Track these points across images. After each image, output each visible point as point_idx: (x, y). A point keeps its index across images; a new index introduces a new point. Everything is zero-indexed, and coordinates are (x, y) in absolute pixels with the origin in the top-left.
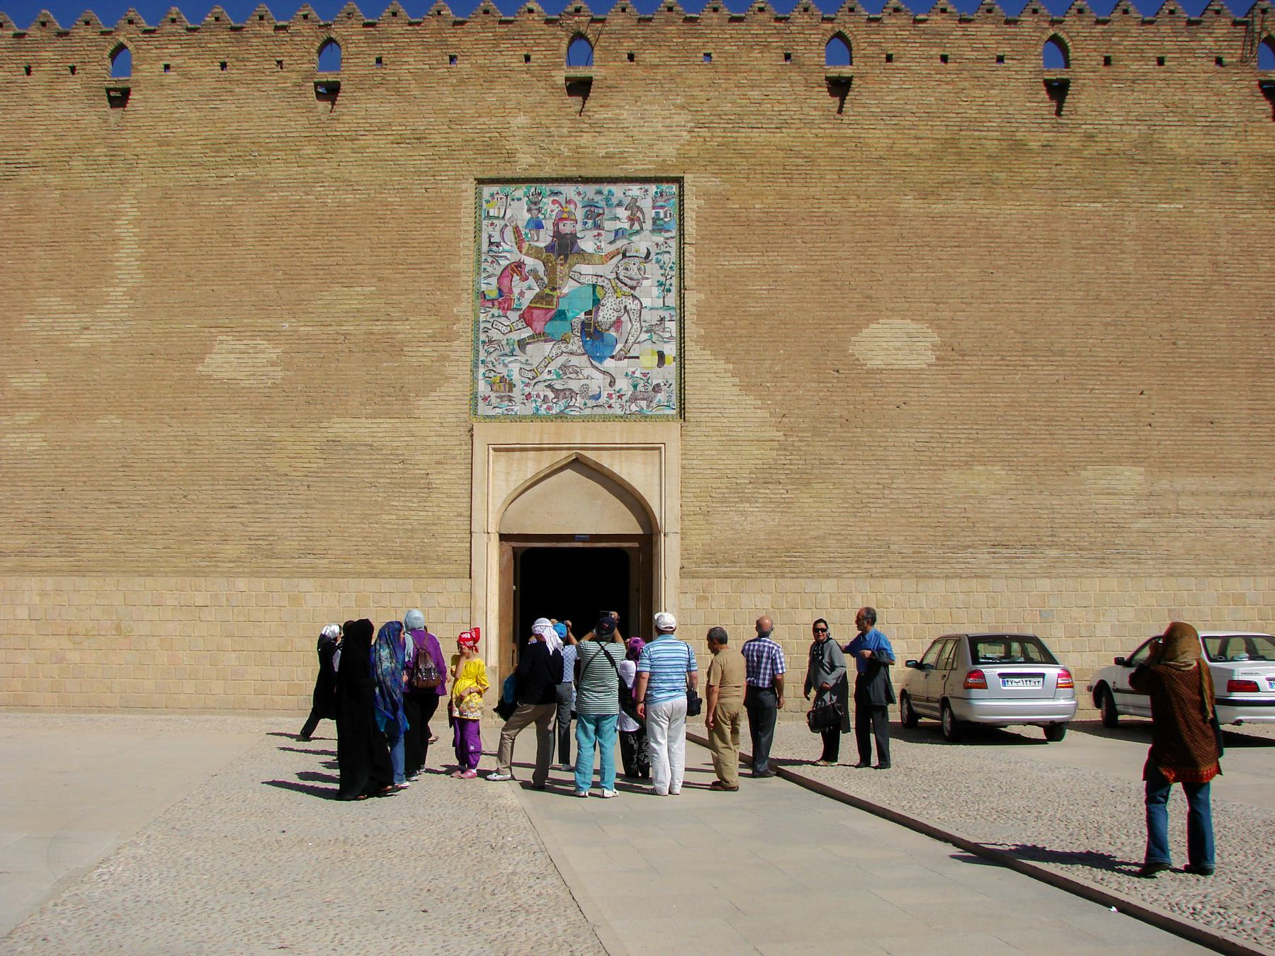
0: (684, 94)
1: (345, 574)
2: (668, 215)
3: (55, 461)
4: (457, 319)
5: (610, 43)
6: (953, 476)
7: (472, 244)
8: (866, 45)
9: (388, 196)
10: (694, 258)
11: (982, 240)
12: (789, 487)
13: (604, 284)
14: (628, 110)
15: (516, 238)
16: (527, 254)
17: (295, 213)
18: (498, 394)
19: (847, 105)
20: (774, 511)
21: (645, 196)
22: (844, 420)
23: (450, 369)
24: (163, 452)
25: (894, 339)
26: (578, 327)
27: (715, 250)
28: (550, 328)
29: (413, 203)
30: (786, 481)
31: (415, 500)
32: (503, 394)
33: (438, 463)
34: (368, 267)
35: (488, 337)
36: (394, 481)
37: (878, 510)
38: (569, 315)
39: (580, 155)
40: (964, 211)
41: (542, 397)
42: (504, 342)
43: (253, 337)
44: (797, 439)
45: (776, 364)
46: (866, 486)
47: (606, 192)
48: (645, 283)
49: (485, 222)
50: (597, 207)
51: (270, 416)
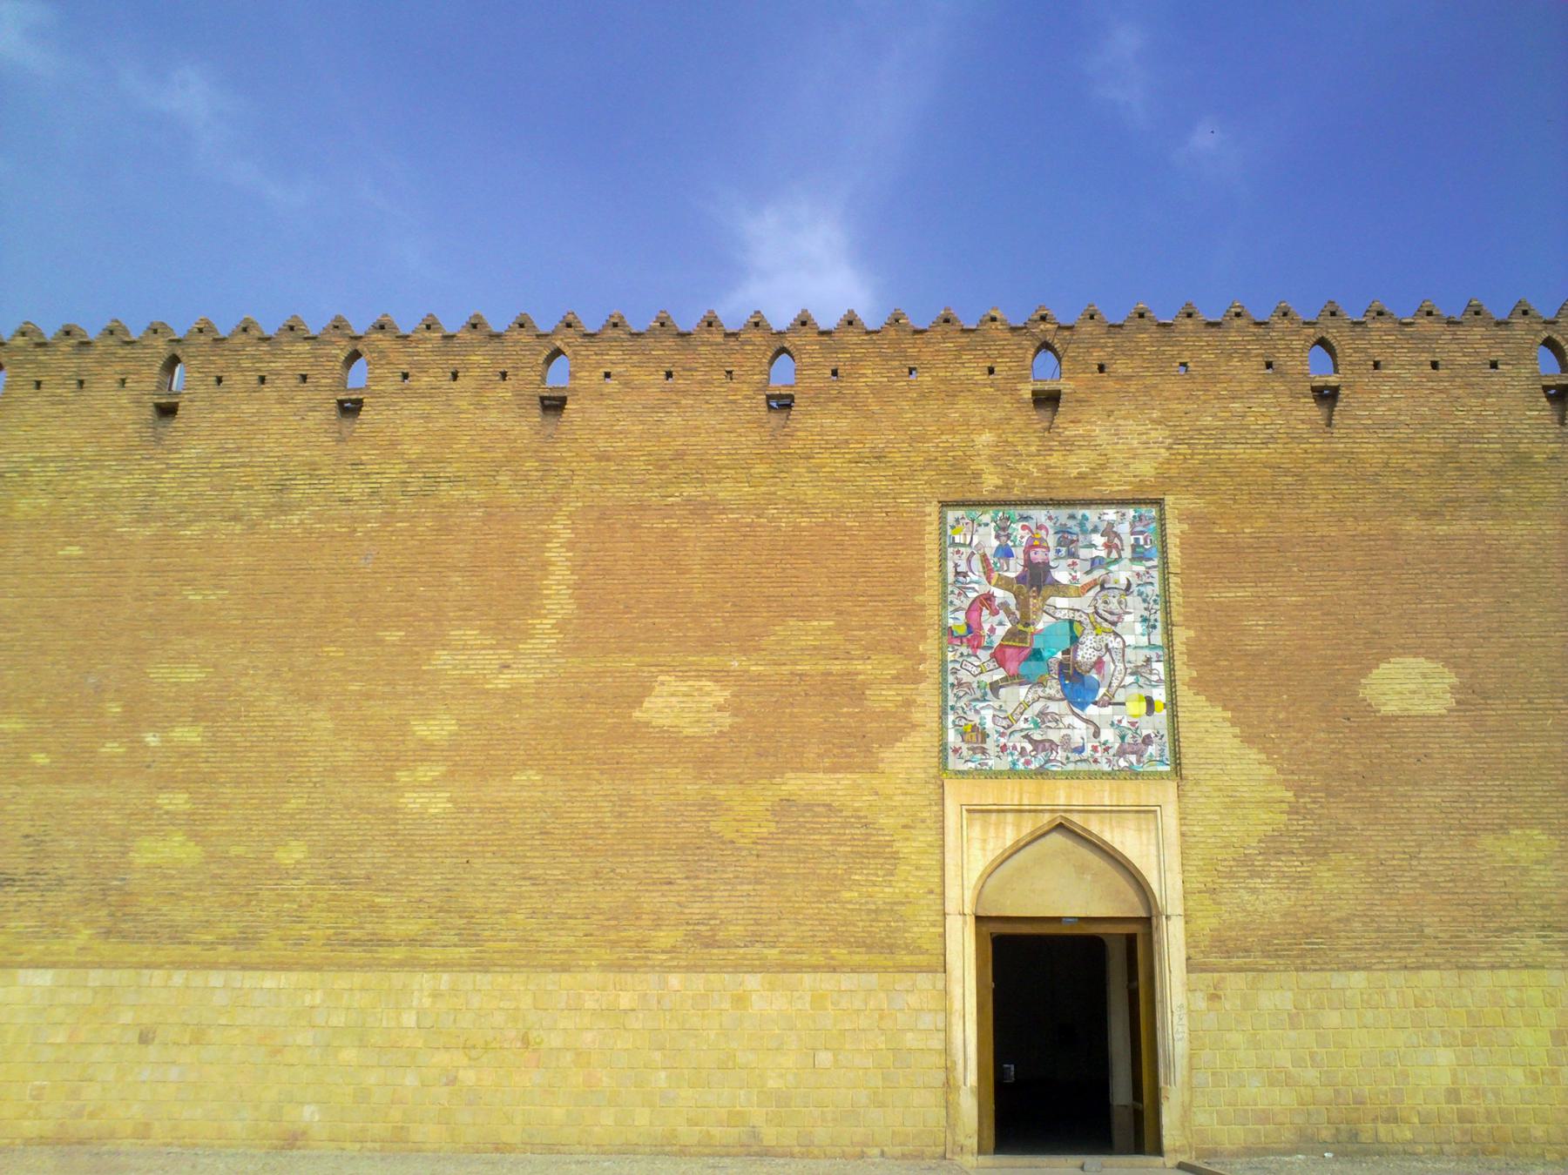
0: (1159, 407)
3: (461, 827)
4: (923, 658)
6: (1487, 841)
7: (937, 574)
10: (1180, 590)
11: (1494, 565)
12: (1305, 858)
13: (1082, 619)
14: (1101, 426)
15: (984, 568)
16: (996, 585)
19: (1336, 419)
20: (1288, 888)
22: (1360, 778)
23: (917, 716)
24: (590, 815)
26: (1055, 668)
27: (1202, 581)
30: (1300, 851)
33: (905, 827)
34: (825, 599)
35: (957, 679)
37: (1407, 885)
38: (1046, 654)
39: (1050, 476)
40: (1471, 532)
41: (1019, 749)
43: (698, 677)
44: (1309, 800)
46: (1391, 856)
48: (1127, 618)
51: (716, 770)
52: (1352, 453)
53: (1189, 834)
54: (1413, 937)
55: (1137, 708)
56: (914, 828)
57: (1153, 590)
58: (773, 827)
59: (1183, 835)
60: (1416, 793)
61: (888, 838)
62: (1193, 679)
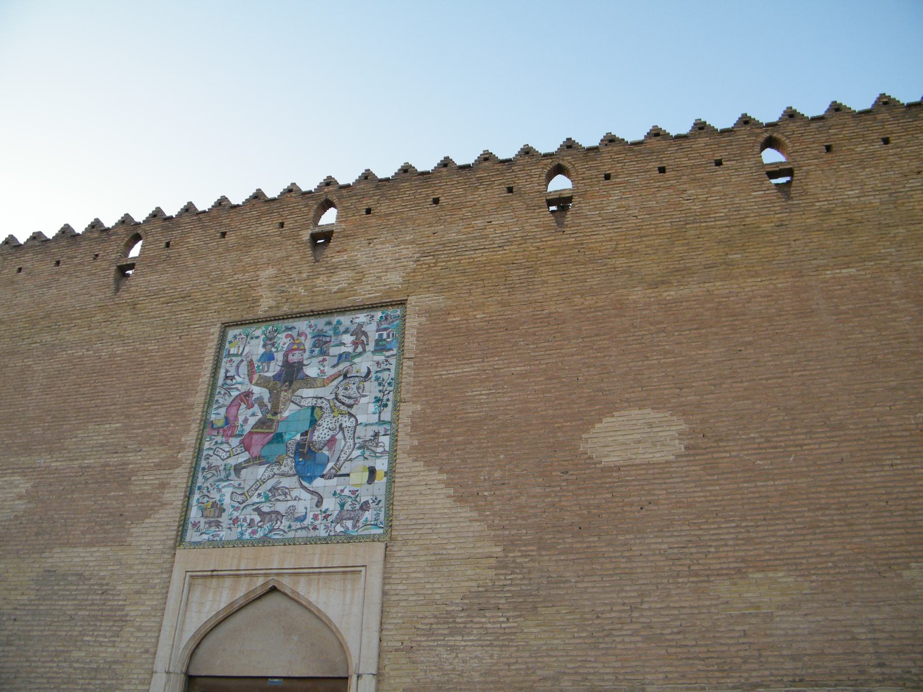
0: (412, 232)
2: (391, 335)
4: (182, 448)
11: (723, 319)
12: (511, 614)
13: (323, 405)
15: (248, 371)
16: (257, 384)
18: (208, 520)
21: (369, 322)
22: (576, 529)
23: (168, 496)
25: (632, 432)
26: (292, 448)
27: (434, 362)
30: (506, 606)
31: (108, 634)
32: (212, 519)
33: (138, 592)
35: (208, 463)
37: (627, 639)
38: (286, 437)
40: (699, 294)
41: (248, 521)
44: (519, 554)
45: (496, 471)
46: (608, 608)
48: (363, 400)
49: (225, 360)
52: (582, 244)
53: (392, 592)
55: (359, 477)
59: (384, 593)
60: (638, 541)
61: (121, 603)
62: (413, 447)
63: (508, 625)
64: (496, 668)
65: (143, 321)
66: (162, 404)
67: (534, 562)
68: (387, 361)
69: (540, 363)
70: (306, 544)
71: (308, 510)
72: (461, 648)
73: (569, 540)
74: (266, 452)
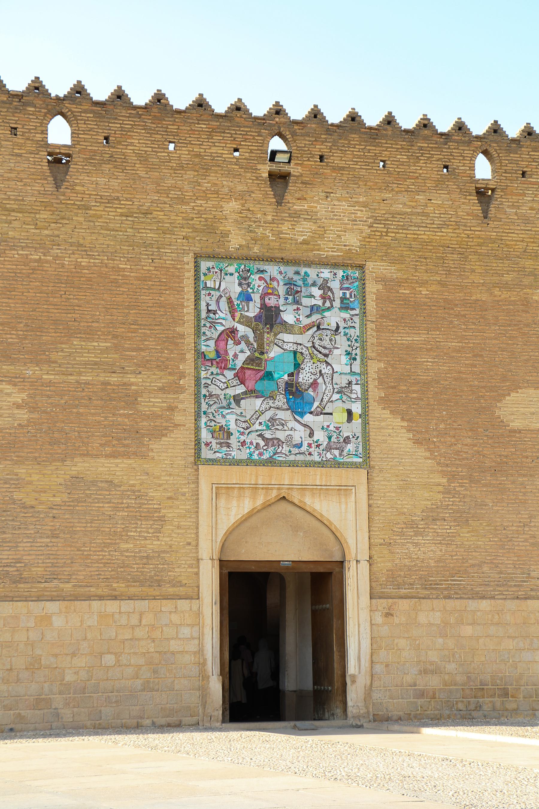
1: (89, 598)
2: (353, 297)
4: (182, 375)
5: (305, 144)
8: (507, 162)
9: (119, 262)
10: (375, 334)
13: (303, 351)
14: (321, 204)
15: (229, 308)
16: (239, 322)
17: (35, 272)
18: (218, 441)
19: (492, 211)
22: (493, 471)
23: (178, 418)
25: (529, 406)
26: (282, 386)
27: (390, 327)
28: (259, 386)
29: (143, 272)
31: (150, 531)
32: (222, 441)
33: (169, 498)
35: (208, 391)
36: (130, 514)
37: (520, 544)
38: (276, 376)
41: (255, 445)
42: (222, 397)
46: (511, 524)
47: (303, 274)
48: (336, 352)
49: (203, 292)
50: (296, 285)
51: (17, 454)
54: (523, 578)
55: (340, 417)
56: (177, 499)
57: (355, 333)
58: (65, 497)
59: (370, 506)
61: (155, 506)
63: (451, 531)
64: (444, 558)
65: (102, 232)
66: (152, 330)
67: (467, 490)
68: (352, 319)
69: (469, 342)
70: (306, 466)
71: (303, 440)
72: (422, 544)
73: (488, 478)
74: (259, 386)
